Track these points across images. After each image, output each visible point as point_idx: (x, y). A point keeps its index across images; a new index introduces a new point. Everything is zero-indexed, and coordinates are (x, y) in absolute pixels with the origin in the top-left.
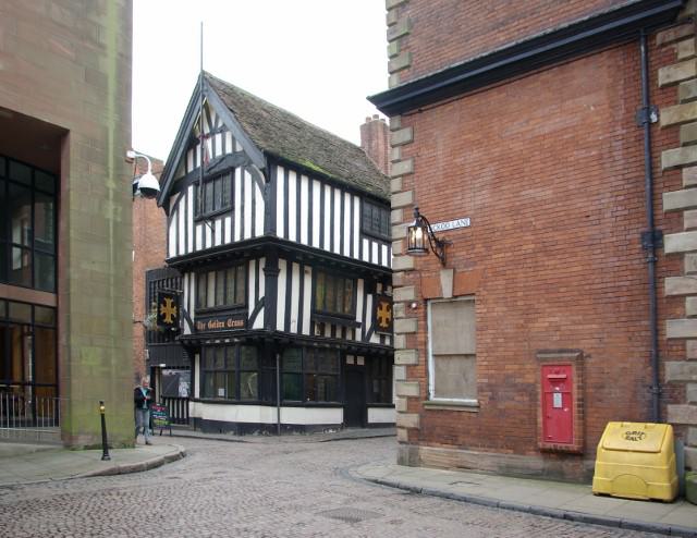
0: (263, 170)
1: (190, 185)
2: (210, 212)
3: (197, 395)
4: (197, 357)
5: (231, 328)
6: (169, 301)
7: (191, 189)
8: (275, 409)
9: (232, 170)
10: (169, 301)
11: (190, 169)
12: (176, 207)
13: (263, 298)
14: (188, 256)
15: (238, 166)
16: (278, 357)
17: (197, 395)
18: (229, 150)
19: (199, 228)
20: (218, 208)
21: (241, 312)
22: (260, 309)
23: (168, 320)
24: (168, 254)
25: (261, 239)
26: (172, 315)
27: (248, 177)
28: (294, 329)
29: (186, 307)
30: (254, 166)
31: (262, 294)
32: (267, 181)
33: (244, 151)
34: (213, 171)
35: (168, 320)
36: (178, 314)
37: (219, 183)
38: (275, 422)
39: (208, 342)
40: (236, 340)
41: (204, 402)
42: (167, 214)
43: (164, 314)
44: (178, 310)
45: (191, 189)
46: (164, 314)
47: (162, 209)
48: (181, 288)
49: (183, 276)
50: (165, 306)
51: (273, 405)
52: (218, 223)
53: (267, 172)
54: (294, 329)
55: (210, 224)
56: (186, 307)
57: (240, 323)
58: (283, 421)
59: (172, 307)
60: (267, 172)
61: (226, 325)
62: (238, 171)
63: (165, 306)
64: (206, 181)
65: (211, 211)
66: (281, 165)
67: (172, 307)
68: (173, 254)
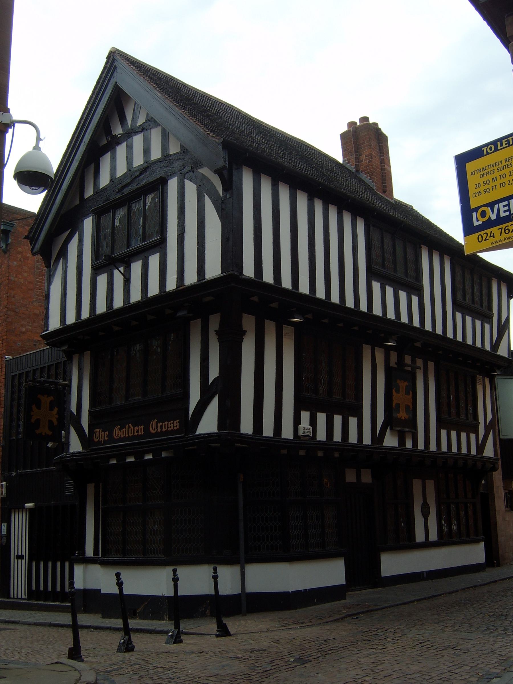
0: (219, 172)
1: (87, 216)
2: (120, 251)
3: (89, 551)
4: (91, 489)
5: (157, 434)
6: (46, 400)
7: (88, 223)
9: (163, 182)
10: (46, 400)
11: (89, 192)
12: (63, 253)
14: (80, 324)
15: (172, 175)
17: (89, 551)
18: (156, 154)
19: (102, 280)
20: (137, 244)
23: (44, 430)
24: (46, 324)
25: (215, 281)
27: (191, 188)
28: (268, 431)
29: (74, 409)
30: (205, 171)
31: (214, 373)
32: (225, 190)
33: (184, 150)
34: (126, 191)
35: (44, 430)
37: (137, 206)
38: (237, 590)
39: (113, 462)
40: (164, 454)
41: (104, 564)
42: (48, 266)
43: (38, 421)
45: (88, 223)
46: (38, 421)
47: (39, 257)
48: (67, 377)
49: (70, 359)
50: (39, 407)
52: (136, 267)
53: (225, 173)
54: (268, 431)
55: (122, 269)
56: (74, 409)
57: (173, 425)
58: (251, 588)
59: (51, 409)
60: (225, 173)
61: (146, 429)
62: (173, 184)
63: (39, 407)
64: (115, 206)
65: (125, 250)
66: (249, 166)
68: (54, 324)
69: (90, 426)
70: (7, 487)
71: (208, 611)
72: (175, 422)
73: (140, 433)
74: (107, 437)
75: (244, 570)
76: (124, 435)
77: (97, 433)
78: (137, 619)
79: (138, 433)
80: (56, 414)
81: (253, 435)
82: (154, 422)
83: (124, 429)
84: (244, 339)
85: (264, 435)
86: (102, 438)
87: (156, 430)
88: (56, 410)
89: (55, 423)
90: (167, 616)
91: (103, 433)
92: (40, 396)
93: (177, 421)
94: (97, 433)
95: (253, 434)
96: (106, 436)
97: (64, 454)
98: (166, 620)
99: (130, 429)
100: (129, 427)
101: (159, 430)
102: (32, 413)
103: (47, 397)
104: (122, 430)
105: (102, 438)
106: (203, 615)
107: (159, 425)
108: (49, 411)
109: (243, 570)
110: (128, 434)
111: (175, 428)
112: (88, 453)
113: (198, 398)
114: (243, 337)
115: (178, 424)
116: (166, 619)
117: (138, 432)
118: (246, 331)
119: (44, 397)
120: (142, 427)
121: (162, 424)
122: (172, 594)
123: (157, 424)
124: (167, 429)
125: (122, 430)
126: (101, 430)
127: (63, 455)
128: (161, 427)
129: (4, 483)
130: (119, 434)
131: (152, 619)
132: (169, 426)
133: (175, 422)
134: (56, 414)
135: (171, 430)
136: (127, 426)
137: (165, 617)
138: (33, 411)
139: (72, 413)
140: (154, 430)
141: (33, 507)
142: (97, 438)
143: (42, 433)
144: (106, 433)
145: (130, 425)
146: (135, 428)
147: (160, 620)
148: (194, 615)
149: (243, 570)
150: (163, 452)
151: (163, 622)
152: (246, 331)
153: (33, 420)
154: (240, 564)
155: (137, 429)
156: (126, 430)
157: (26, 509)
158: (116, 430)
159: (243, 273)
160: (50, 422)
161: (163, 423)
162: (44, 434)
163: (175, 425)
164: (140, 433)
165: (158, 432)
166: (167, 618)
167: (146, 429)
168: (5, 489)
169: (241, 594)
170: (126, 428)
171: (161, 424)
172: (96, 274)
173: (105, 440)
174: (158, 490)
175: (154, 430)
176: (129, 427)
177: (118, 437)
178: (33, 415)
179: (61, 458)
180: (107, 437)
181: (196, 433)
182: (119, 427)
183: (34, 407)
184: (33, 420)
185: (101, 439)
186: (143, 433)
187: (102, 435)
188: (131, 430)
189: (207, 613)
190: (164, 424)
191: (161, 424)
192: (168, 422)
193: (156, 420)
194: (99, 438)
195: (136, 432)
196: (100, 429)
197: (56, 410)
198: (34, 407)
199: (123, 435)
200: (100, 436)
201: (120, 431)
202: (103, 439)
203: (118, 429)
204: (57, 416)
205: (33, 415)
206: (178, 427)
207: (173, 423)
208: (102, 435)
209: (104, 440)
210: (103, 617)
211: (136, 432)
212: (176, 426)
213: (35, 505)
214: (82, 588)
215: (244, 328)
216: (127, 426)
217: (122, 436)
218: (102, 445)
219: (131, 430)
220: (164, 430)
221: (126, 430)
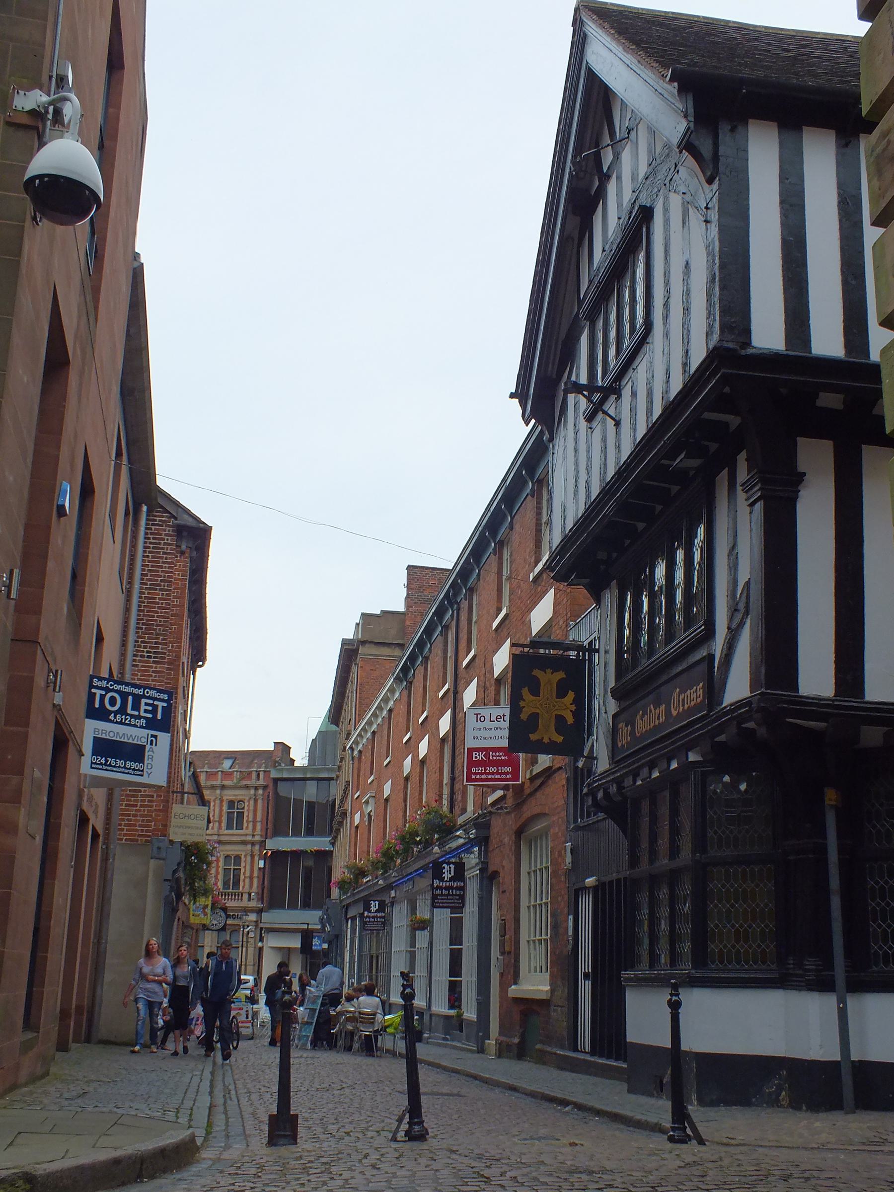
6: (549, 679)
8: (830, 1001)
13: (748, 584)
16: (831, 796)
21: (703, 653)
22: (741, 624)
36: (578, 714)
40: (692, 757)
43: (535, 717)
46: (535, 717)
50: (535, 692)
51: (824, 985)
59: (561, 694)
61: (668, 712)
63: (535, 692)
67: (561, 693)
70: (572, 851)
75: (839, 1006)
80: (571, 704)
81: (834, 698)
84: (800, 491)
85: (869, 697)
88: (571, 695)
89: (570, 720)
92: (537, 673)
93: (701, 684)
95: (835, 696)
100: (651, 711)
102: (522, 704)
106: (774, 1102)
108: (557, 698)
109: (841, 1005)
110: (650, 725)
111: (699, 700)
114: (799, 488)
118: (804, 474)
119: (546, 673)
122: (669, 1045)
123: (679, 698)
129: (567, 844)
132: (692, 698)
134: (571, 704)
140: (676, 710)
141: (594, 884)
143: (543, 738)
148: (754, 1100)
149: (841, 1005)
150: (690, 753)
152: (804, 474)
154: (835, 992)
157: (589, 888)
159: (751, 343)
160: (560, 719)
162: (546, 740)
167: (668, 712)
168: (570, 855)
169: (839, 1061)
172: (591, 428)
181: (722, 704)
183: (525, 692)
184: (524, 716)
186: (664, 717)
189: (780, 1098)
197: (571, 695)
204: (573, 708)
209: (627, 743)
210: (630, 1091)
212: (700, 697)
213: (598, 880)
215: (801, 468)
218: (627, 750)
220: (686, 706)
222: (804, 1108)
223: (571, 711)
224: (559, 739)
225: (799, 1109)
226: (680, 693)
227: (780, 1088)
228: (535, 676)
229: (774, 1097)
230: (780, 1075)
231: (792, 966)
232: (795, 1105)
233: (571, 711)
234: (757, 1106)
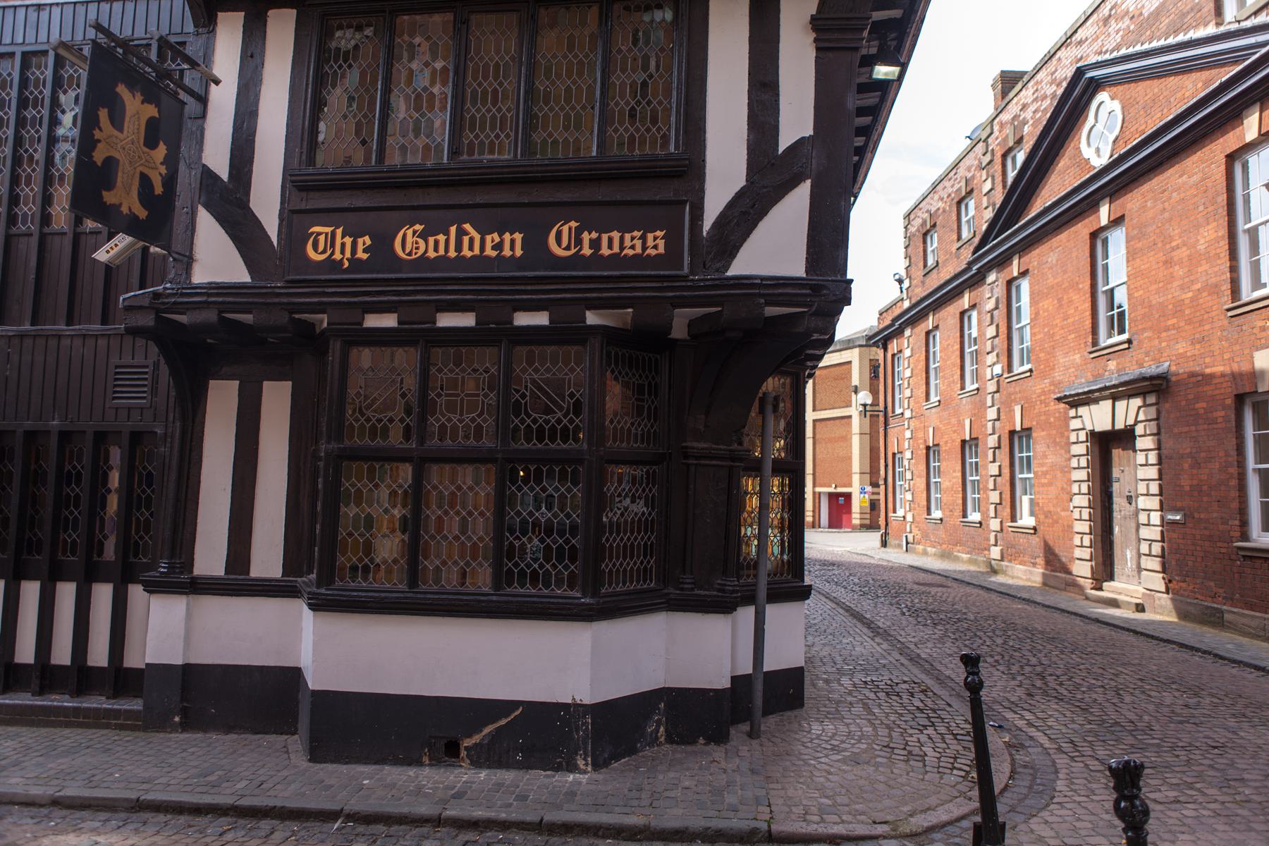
10: (137, 109)
21: (666, 192)
26: (145, 181)
43: (110, 162)
44: (172, 161)
59: (151, 143)
61: (535, 244)
69: (288, 215)
71: (662, 729)
72: (650, 236)
73: (507, 252)
74: (365, 251)
76: (442, 252)
77: (322, 238)
78: (461, 766)
79: (502, 250)
80: (161, 164)
82: (565, 229)
83: (441, 238)
86: (343, 252)
87: (573, 251)
90: (589, 759)
91: (348, 240)
94: (322, 238)
96: (360, 247)
97: (168, 285)
98: (585, 772)
99: (466, 239)
100: (461, 233)
101: (587, 251)
102: (97, 134)
103: (143, 103)
104: (431, 240)
105: (343, 252)
106: (654, 741)
107: (586, 236)
112: (278, 291)
113: (740, 181)
115: (661, 243)
116: (582, 767)
117: (498, 247)
120: (518, 237)
121: (599, 238)
124: (616, 249)
125: (431, 240)
126: (339, 232)
127: (165, 289)
128: (595, 244)
130: (417, 248)
131: (526, 766)
133: (650, 236)
134: (161, 164)
135: (635, 256)
136: (453, 229)
137: (581, 763)
138: (100, 129)
139: (208, 175)
140: (568, 248)
142: (324, 252)
144: (360, 241)
145: (467, 227)
146: (489, 238)
147: (558, 768)
151: (571, 777)
153: (99, 156)
155: (497, 239)
156: (447, 242)
158: (405, 236)
160: (145, 181)
161: (600, 232)
162: (125, 210)
163: (650, 243)
164: (507, 252)
165: (583, 256)
166: (587, 765)
167: (535, 244)
170: (447, 233)
171: (594, 235)
173: (360, 260)
174: (559, 415)
175: (568, 248)
176: (461, 233)
177: (414, 257)
178: (99, 141)
179: (156, 295)
180: (365, 251)
182: (419, 227)
185: (338, 256)
186: (519, 252)
187: (343, 245)
188: (472, 240)
189: (659, 734)
190: (605, 237)
191: (594, 235)
192: (624, 230)
193: (574, 224)
194: (333, 253)
195: (493, 248)
196: (338, 227)
198: (103, 114)
199: (436, 250)
200: (333, 245)
201: (421, 242)
202: (348, 255)
203: (415, 232)
204: (163, 170)
205: (99, 141)
206: (661, 250)
207: (643, 238)
208: (343, 245)
211: (493, 248)
214: (180, 662)
216: (453, 229)
217: (432, 254)
219: (472, 240)
220: (605, 251)
221: (447, 242)
222: (701, 741)
223: (160, 174)
224: (142, 214)
225: (693, 742)
226: (579, 231)
227: (659, 723)
228: (117, 95)
229: (654, 735)
230: (659, 709)
231: (689, 586)
232: (670, 740)
233: (160, 174)
234: (642, 751)
